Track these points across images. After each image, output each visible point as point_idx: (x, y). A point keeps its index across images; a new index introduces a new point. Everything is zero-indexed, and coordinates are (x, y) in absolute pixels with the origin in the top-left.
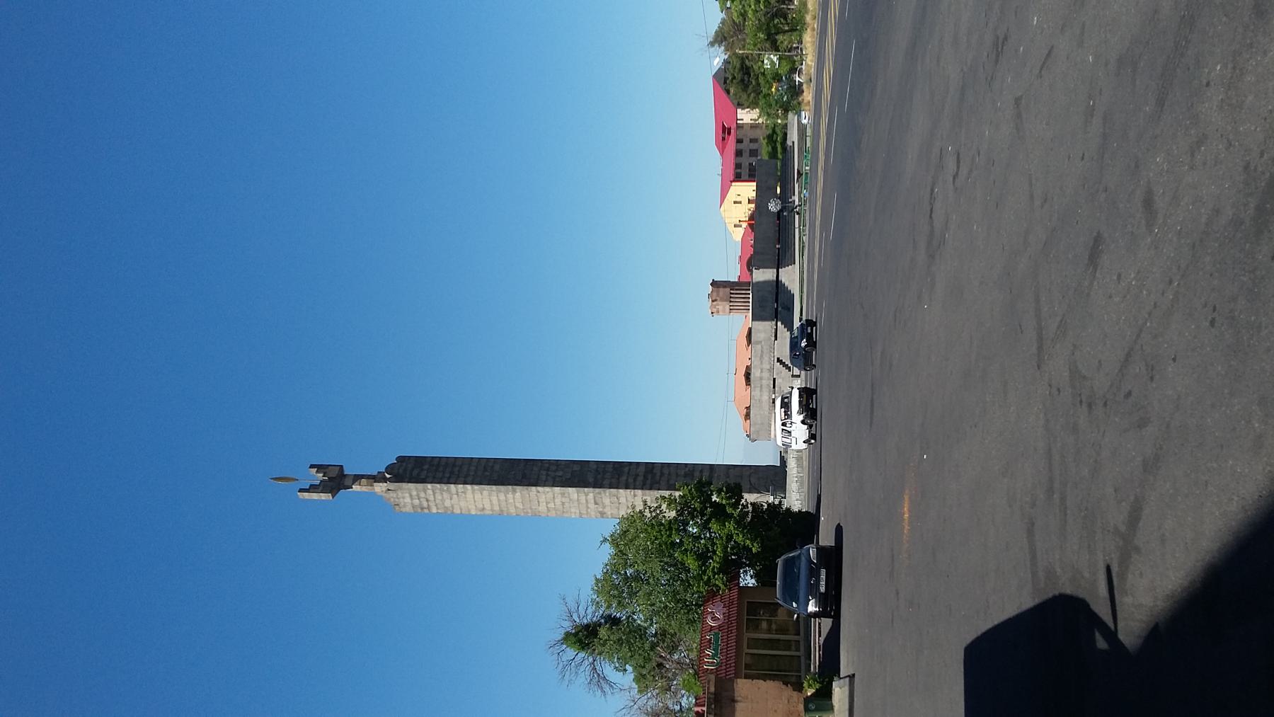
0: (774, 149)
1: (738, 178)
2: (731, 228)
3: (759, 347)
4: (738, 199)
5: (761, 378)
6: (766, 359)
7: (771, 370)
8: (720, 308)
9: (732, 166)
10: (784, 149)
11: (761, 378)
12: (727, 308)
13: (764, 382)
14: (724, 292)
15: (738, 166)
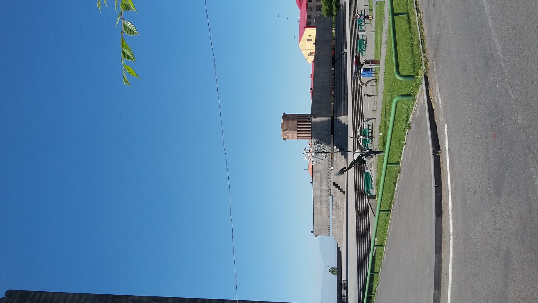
0: (331, 8)
1: (309, 25)
2: (306, 55)
3: (319, 175)
4: (310, 38)
5: (321, 196)
6: (325, 183)
7: (329, 191)
8: (290, 135)
9: (305, 18)
10: (338, 7)
11: (321, 196)
12: (295, 135)
13: (323, 198)
14: (293, 123)
15: (309, 17)
